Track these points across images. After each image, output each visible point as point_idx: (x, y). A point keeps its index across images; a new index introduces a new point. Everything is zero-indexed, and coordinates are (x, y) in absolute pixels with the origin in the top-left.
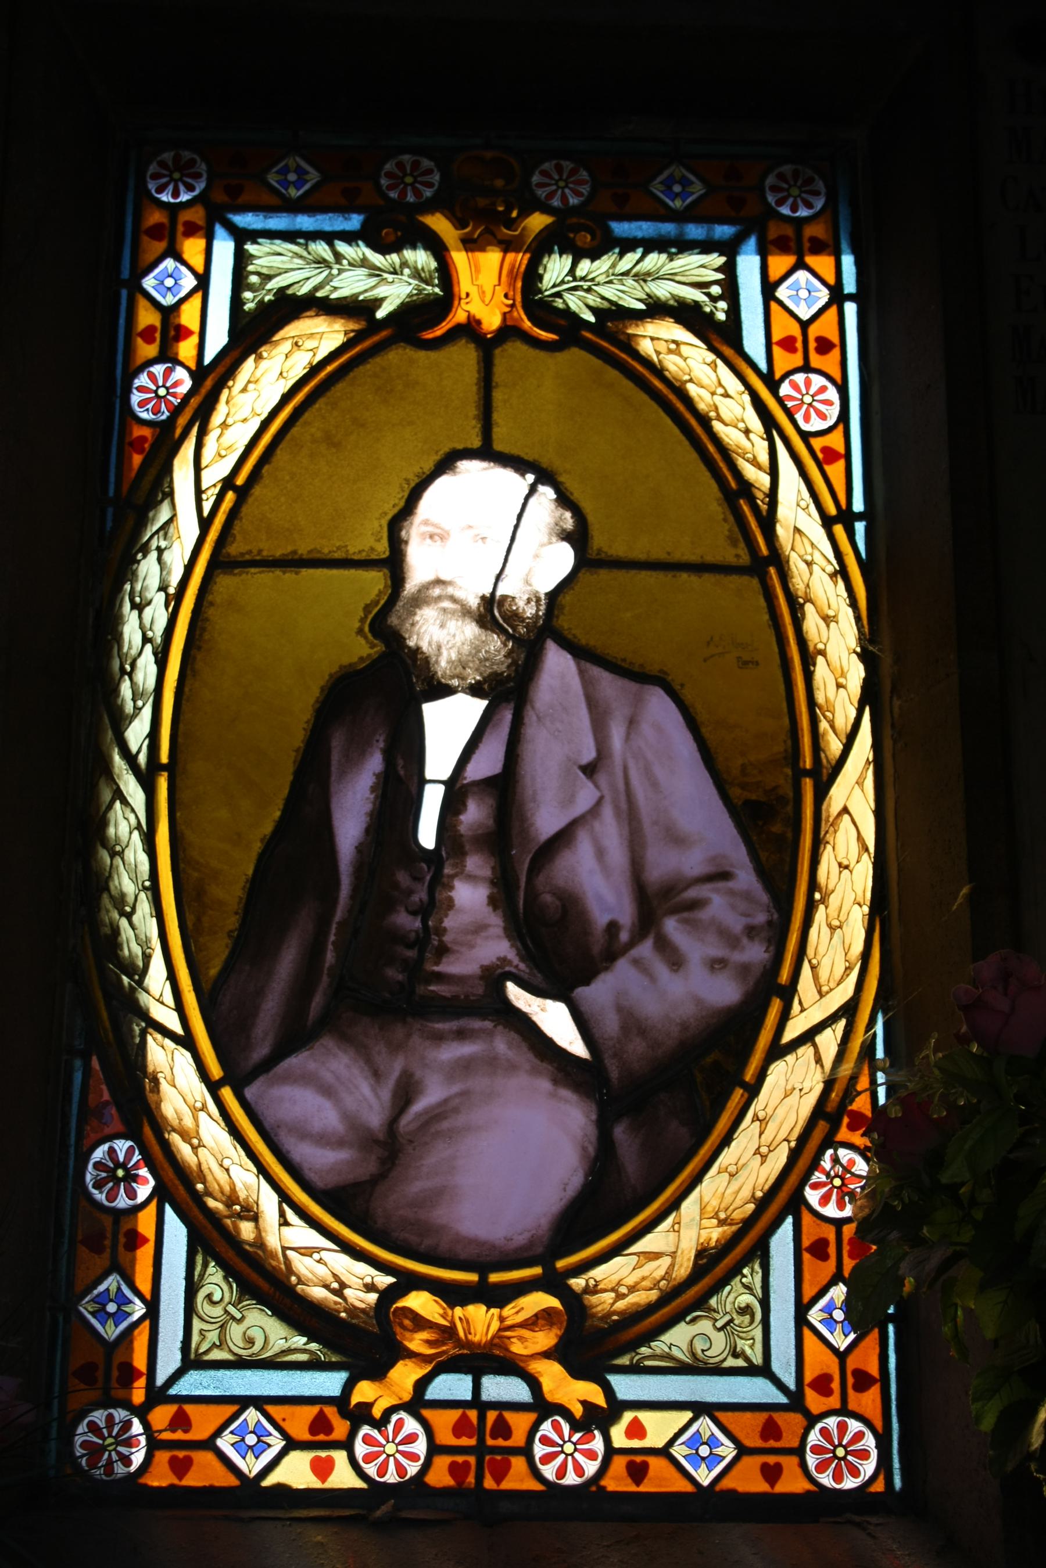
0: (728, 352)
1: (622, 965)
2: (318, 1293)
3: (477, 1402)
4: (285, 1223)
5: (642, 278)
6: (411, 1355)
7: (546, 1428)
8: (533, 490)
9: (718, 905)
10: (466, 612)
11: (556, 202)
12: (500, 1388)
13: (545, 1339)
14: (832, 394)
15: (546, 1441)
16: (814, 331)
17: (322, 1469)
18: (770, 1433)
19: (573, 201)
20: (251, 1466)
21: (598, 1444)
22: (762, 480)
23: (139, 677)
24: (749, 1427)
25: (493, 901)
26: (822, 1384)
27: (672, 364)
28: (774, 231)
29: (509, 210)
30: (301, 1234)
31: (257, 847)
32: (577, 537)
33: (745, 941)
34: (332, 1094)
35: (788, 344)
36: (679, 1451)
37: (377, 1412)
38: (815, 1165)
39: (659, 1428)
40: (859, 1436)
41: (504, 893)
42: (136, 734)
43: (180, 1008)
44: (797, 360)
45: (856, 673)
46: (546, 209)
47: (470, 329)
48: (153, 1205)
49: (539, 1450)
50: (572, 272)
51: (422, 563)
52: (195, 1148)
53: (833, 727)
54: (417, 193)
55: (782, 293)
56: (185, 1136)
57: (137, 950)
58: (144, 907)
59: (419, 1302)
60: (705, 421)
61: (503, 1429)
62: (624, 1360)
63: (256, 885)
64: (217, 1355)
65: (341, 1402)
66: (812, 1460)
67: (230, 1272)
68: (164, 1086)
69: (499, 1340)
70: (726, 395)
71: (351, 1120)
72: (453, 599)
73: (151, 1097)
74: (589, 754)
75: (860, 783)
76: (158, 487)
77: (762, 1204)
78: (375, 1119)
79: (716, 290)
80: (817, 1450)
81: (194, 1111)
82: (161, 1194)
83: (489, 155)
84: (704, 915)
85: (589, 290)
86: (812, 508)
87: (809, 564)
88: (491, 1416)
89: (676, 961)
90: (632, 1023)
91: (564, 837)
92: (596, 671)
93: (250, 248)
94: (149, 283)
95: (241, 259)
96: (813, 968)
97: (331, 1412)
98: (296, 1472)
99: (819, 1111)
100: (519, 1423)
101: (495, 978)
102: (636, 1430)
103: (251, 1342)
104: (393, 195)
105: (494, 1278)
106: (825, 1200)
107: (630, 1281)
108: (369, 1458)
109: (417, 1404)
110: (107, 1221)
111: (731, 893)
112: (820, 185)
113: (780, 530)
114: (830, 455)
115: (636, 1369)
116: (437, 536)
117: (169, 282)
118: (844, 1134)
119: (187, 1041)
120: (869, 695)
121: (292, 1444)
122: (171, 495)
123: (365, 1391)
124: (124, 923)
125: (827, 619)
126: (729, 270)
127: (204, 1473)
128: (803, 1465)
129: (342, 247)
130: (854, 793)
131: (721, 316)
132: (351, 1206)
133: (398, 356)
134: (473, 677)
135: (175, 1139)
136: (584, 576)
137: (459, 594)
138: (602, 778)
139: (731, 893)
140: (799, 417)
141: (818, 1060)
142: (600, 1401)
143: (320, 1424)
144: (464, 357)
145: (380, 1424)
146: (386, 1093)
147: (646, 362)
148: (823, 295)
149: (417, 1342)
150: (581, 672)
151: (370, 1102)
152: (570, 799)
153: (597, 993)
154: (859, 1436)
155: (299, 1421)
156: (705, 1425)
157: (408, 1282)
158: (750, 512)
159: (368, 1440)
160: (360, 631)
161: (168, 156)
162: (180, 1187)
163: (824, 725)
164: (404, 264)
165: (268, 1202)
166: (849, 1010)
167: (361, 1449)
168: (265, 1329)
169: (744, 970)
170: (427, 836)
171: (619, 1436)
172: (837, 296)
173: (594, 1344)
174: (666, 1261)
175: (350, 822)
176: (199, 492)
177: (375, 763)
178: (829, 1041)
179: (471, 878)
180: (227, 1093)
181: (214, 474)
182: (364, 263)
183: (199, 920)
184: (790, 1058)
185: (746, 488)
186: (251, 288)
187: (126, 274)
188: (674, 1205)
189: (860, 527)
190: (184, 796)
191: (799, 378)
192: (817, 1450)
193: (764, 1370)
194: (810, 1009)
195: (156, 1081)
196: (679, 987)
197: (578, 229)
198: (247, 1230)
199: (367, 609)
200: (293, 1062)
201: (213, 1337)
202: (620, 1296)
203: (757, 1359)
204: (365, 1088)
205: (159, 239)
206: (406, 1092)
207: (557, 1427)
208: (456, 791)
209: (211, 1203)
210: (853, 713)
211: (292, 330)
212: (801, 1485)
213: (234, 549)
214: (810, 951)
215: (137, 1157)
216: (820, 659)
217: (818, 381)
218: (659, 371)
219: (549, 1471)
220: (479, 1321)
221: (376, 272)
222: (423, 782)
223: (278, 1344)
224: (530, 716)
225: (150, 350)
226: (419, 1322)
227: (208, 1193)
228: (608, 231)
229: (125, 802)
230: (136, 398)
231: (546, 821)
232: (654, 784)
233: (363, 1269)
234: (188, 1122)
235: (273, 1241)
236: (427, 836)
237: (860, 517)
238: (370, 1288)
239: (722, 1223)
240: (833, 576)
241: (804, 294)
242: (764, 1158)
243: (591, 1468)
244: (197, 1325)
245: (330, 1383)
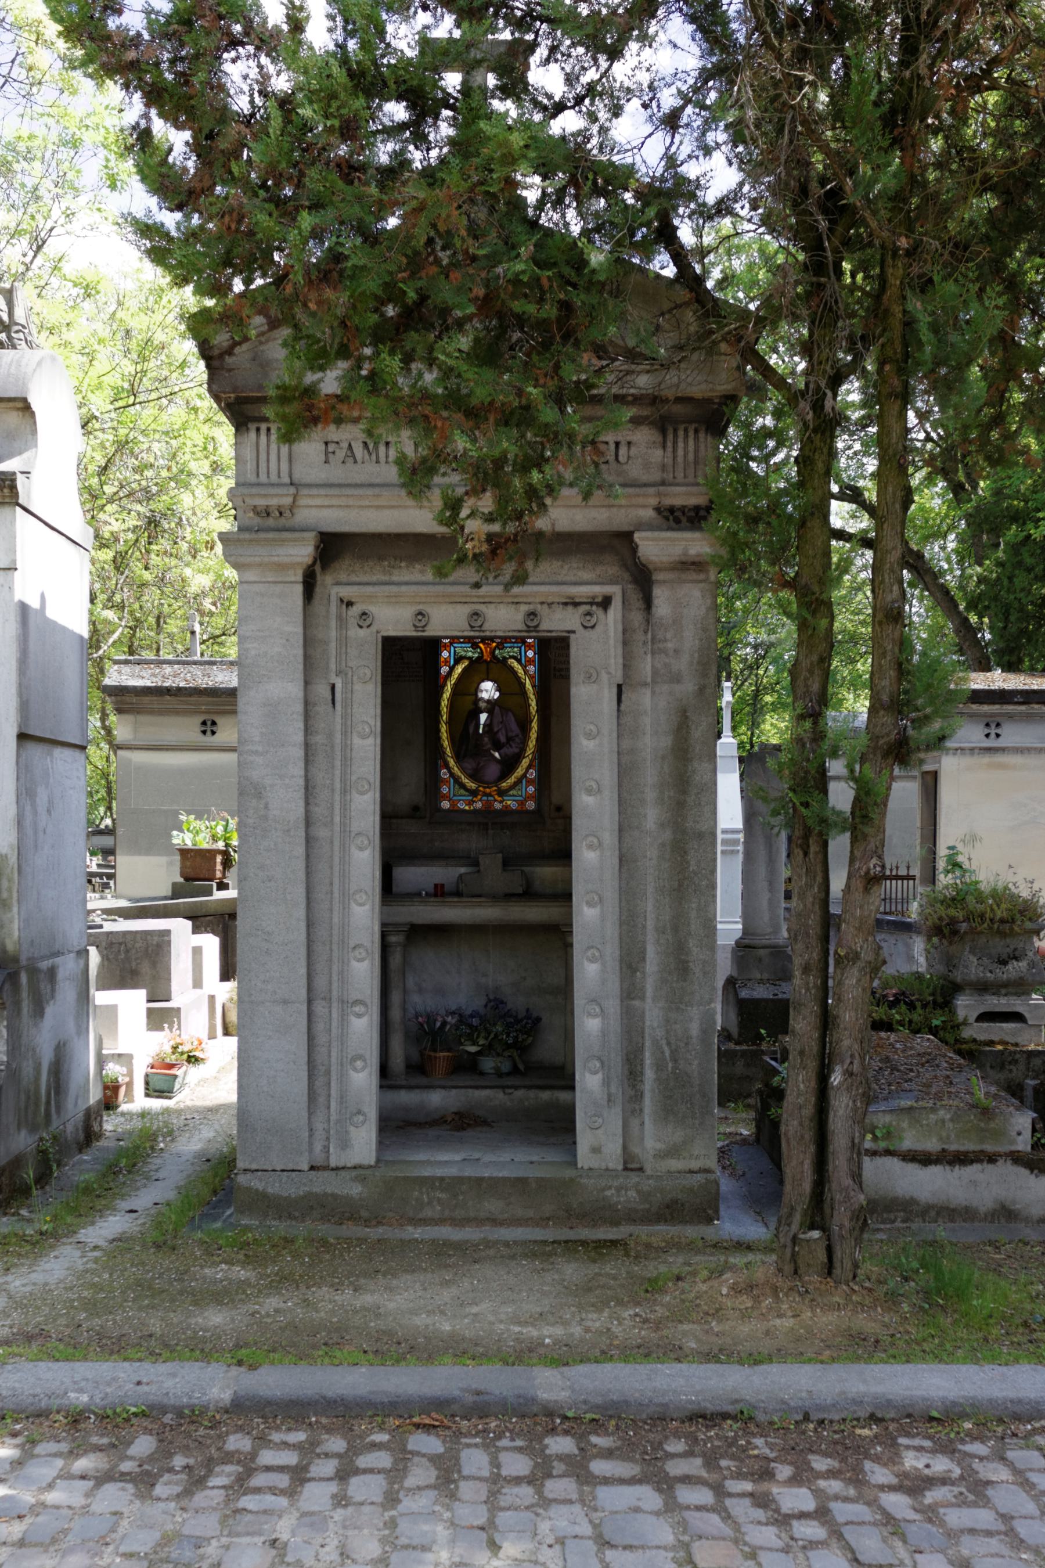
18: (522, 803)
34: (470, 764)
130: (535, 725)
132: (473, 777)
158: (523, 685)
162: (452, 775)
194: (529, 752)
196: (513, 750)
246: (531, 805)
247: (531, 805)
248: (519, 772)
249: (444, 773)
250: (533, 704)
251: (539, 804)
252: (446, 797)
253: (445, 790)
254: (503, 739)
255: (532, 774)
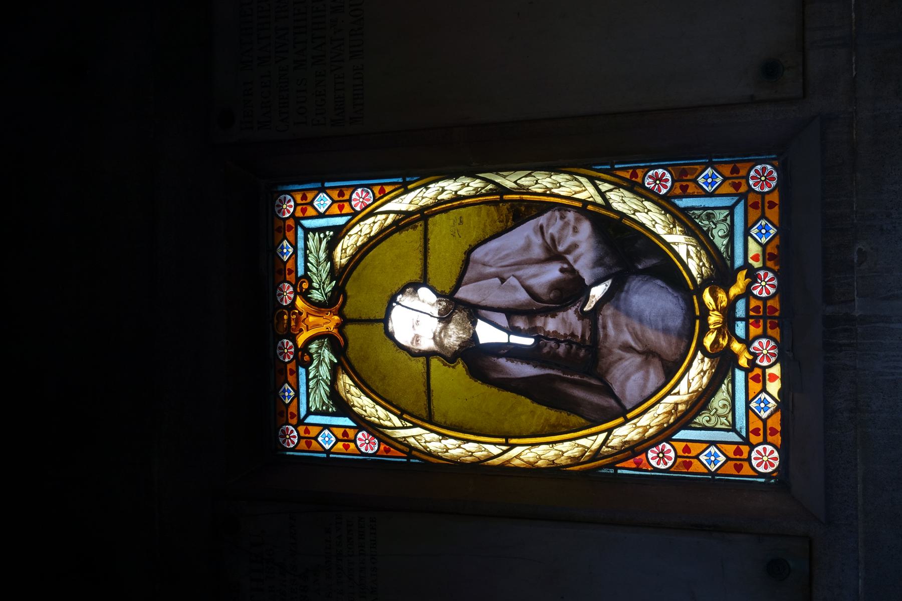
0: (345, 230)
1: (576, 267)
2: (705, 380)
3: (746, 319)
4: (678, 393)
5: (318, 263)
6: (729, 344)
7: (756, 292)
8: (398, 303)
9: (553, 230)
10: (445, 328)
11: (292, 296)
12: (740, 311)
13: (722, 295)
14: (359, 190)
15: (761, 292)
16: (336, 198)
17: (773, 378)
18: (756, 206)
19: (291, 289)
20: (772, 404)
21: (762, 273)
22: (392, 217)
23: (473, 450)
24: (754, 214)
25: (554, 316)
26: (737, 186)
27: (350, 252)
28: (299, 214)
29: (295, 313)
30: (683, 387)
31: (535, 405)
32: (414, 286)
33: (566, 220)
34: (628, 376)
35: (341, 208)
36: (764, 240)
37: (751, 357)
38: (651, 191)
39: (754, 249)
40: (756, 171)
41: (551, 312)
42: (495, 450)
43: (597, 433)
44: (346, 205)
45: (464, 180)
46: (294, 299)
47: (340, 327)
48: (672, 443)
49: (764, 295)
50: (317, 290)
51: (427, 344)
52: (651, 427)
53: (483, 188)
54: (291, 347)
55: (322, 210)
56: (646, 431)
57: (576, 449)
58: (559, 447)
59: (708, 341)
60: (371, 239)
61: (756, 309)
62: (729, 263)
63: (550, 406)
64: (730, 418)
65: (747, 371)
66: (766, 189)
67: (698, 414)
68: (627, 439)
69: (722, 311)
70: (361, 231)
71: (639, 368)
72: (440, 333)
73: (632, 444)
74: (497, 281)
75: (505, 177)
76: (403, 443)
77: (667, 211)
78: (638, 359)
79: (322, 235)
80: (762, 188)
81: (636, 427)
82: (669, 440)
83: (276, 321)
84: (556, 236)
85: (324, 283)
86: (402, 197)
87: (423, 198)
88: (752, 313)
89: (574, 246)
90: (598, 262)
91: (529, 290)
92: (465, 279)
93: (313, 409)
94: (327, 447)
95: (317, 413)
96: (576, 193)
97: (751, 375)
98: (774, 387)
99: (630, 189)
100: (753, 303)
101: (582, 315)
102: (755, 258)
103: (724, 406)
104: (292, 357)
105: (698, 313)
106: (665, 187)
107: (697, 261)
108: (769, 360)
109: (747, 342)
110: (679, 460)
111: (548, 225)
112: (282, 197)
113: (411, 209)
114: (382, 191)
115: (732, 258)
116: (417, 338)
117: (327, 439)
118: (639, 180)
119: (610, 431)
120: (473, 175)
121: (764, 390)
122: (405, 438)
123: (743, 362)
124: (565, 455)
125: (443, 191)
126: (315, 230)
127: (775, 422)
128: (768, 193)
129: (311, 376)
131: (332, 233)
132: (671, 368)
133: (351, 354)
134: (469, 325)
135: (647, 434)
136: (431, 283)
137: (438, 330)
138: (505, 276)
139: (548, 225)
140: (368, 203)
141: (611, 190)
142: (745, 272)
143: (756, 379)
144: (350, 329)
145: (755, 356)
146: (628, 355)
147: (349, 261)
148: (322, 195)
149: (724, 343)
150: (466, 284)
151: (632, 361)
152: (514, 288)
153: (587, 278)
154: (756, 171)
155: (755, 387)
156: (754, 231)
157: (700, 346)
158: (404, 221)
159: (761, 361)
160: (453, 367)
161: (281, 440)
162: (665, 433)
163: (483, 191)
164: (317, 352)
165: (671, 399)
166: (592, 180)
167: (765, 363)
168: (720, 400)
169: (577, 220)
170: (529, 341)
171: (756, 265)
172: (323, 190)
173: (722, 273)
174: (690, 248)
175: (527, 370)
176: (403, 428)
177: (502, 361)
178: (604, 187)
179: (545, 324)
180: (629, 416)
181: (397, 422)
182: (317, 367)
183: (564, 426)
184: (611, 201)
185: (395, 222)
186: (328, 409)
187: (324, 455)
188: (668, 245)
189: (408, 179)
190: (517, 432)
191: (353, 203)
192: (762, 188)
193: (731, 209)
195: (625, 442)
197: (301, 288)
198: (681, 407)
199: (445, 365)
200: (616, 390)
201: (723, 420)
202: (704, 265)
203: (726, 212)
204: (627, 363)
205: (311, 443)
206: (627, 348)
207: (755, 288)
208: (512, 330)
209: (671, 421)
210: (478, 181)
211: (343, 394)
212: (776, 193)
213: (424, 414)
214: (569, 194)
215: (654, 449)
216: (459, 193)
217: (354, 196)
218: (353, 256)
219: (772, 291)
220: (714, 318)
221: (320, 363)
222: (509, 343)
223: (725, 395)
224: (483, 303)
225: (352, 445)
226: (716, 342)
227: (668, 422)
228: (302, 277)
229: (520, 454)
230: (370, 451)
231: (522, 296)
232: (507, 255)
233: (696, 362)
234: (640, 430)
235: (686, 398)
236: (529, 341)
237: (404, 179)
238: (703, 361)
239: (674, 226)
240: (427, 189)
241: (322, 202)
242: (649, 210)
243: (770, 275)
244: (718, 426)
245: (740, 375)
246: (763, 177)
247: (763, 177)
248: (652, 218)
249: (660, 459)
250: (451, 187)
251: (753, 151)
252: (738, 460)
253: (712, 460)
254: (553, 272)
255: (659, 178)
